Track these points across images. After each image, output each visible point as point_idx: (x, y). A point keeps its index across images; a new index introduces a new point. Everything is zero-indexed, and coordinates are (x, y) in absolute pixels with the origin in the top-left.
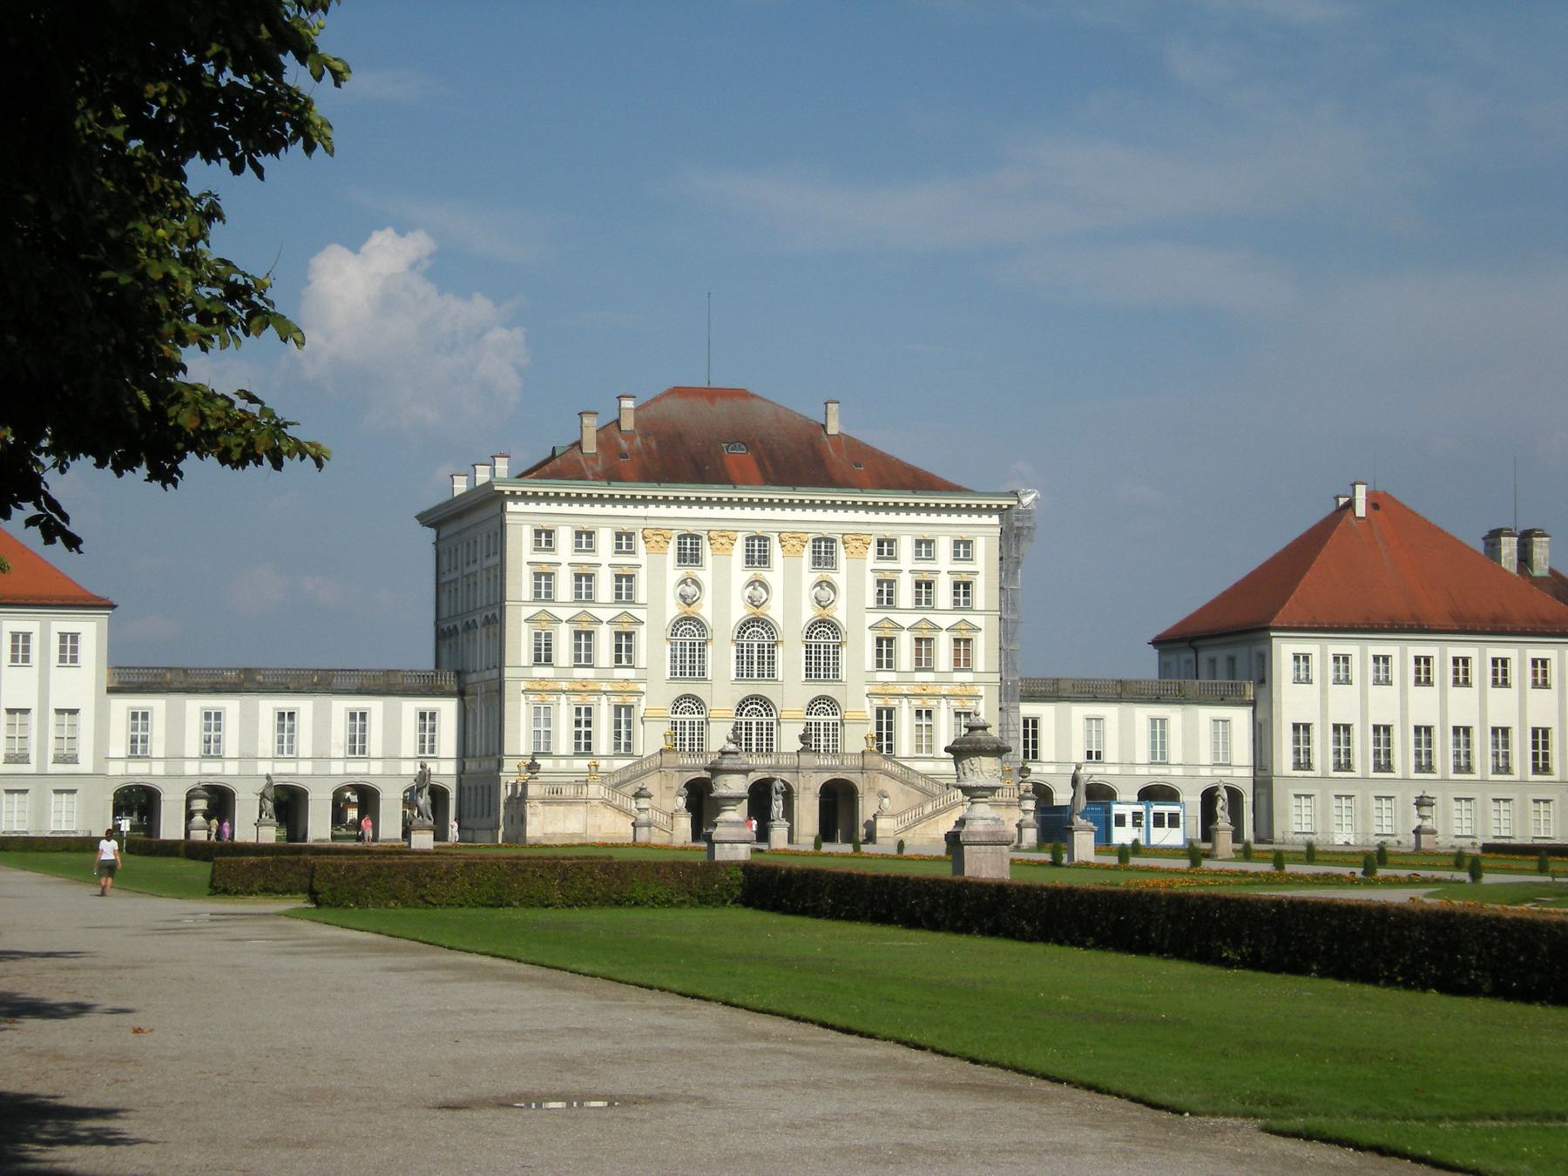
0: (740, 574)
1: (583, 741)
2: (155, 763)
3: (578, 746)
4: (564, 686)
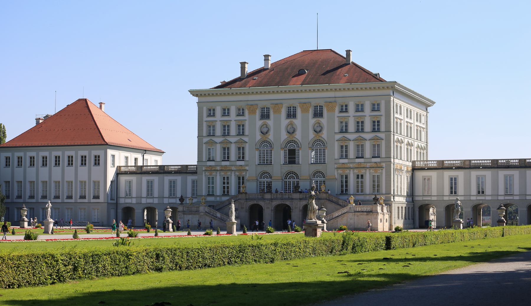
0: (285, 122)
3: (224, 192)
4: (218, 168)
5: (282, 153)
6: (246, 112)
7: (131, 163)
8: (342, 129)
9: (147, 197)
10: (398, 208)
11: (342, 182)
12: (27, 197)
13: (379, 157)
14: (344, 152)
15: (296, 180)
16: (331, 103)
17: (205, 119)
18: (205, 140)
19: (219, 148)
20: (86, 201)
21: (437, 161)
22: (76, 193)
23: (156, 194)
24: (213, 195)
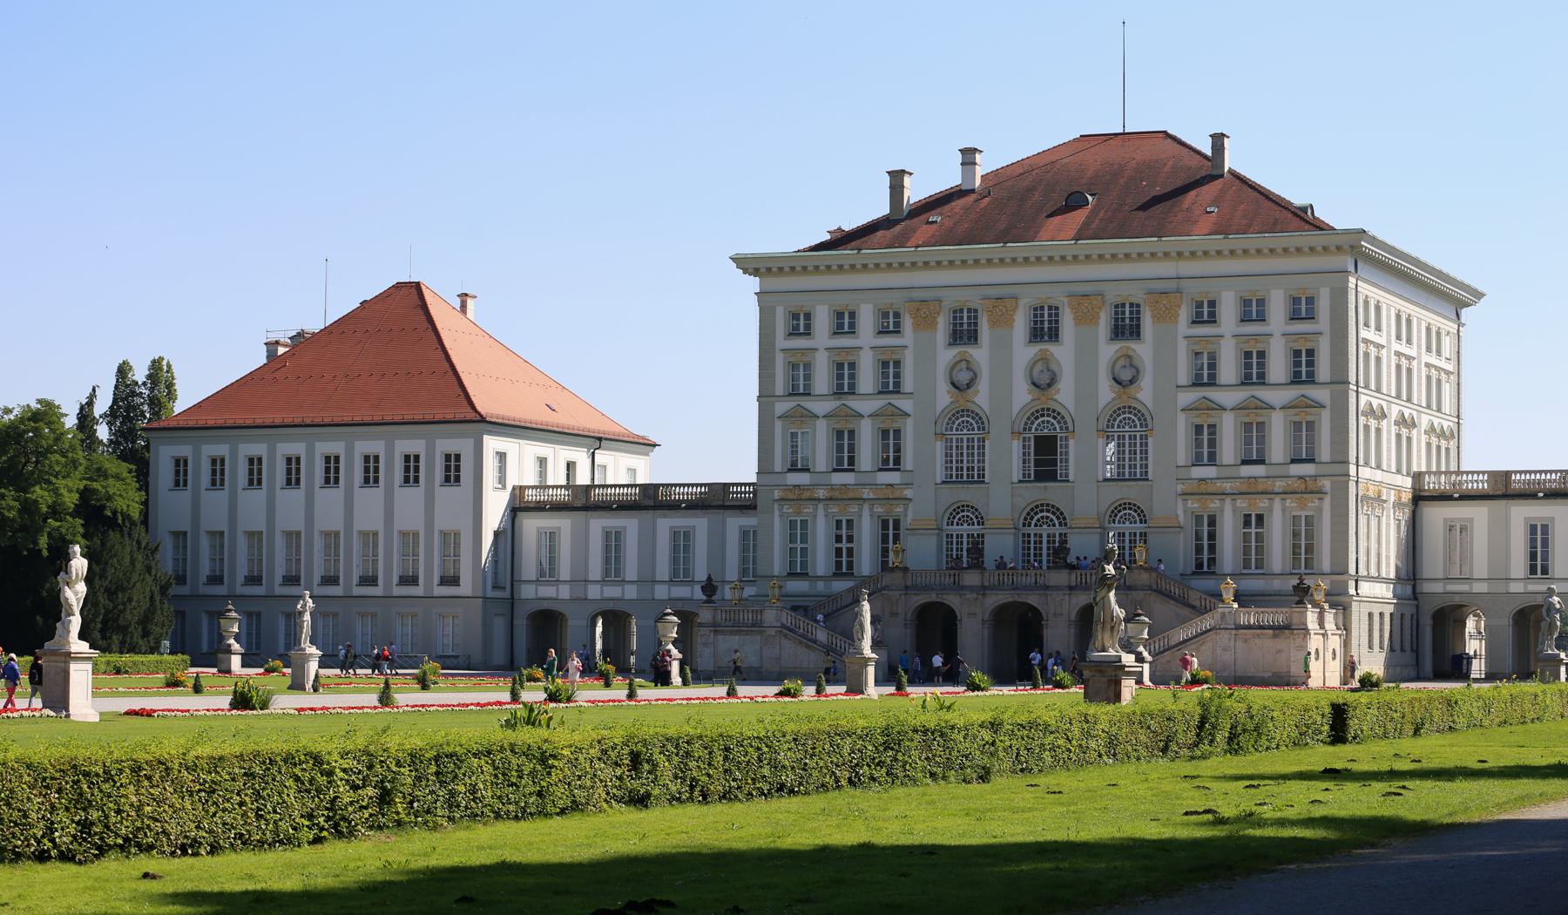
0: (1023, 353)
1: (844, 559)
2: (561, 587)
3: (839, 564)
4: (821, 493)
5: (1016, 445)
6: (907, 323)
7: (557, 476)
8: (1198, 376)
9: (603, 582)
10: (1370, 615)
11: (1198, 537)
12: (240, 579)
13: (1312, 461)
14: (1205, 445)
15: (1057, 530)
16: (1165, 296)
17: (781, 342)
18: (782, 407)
19: (822, 431)
20: (418, 591)
21: (1490, 473)
22: (389, 568)
23: (631, 571)
24: (804, 575)
